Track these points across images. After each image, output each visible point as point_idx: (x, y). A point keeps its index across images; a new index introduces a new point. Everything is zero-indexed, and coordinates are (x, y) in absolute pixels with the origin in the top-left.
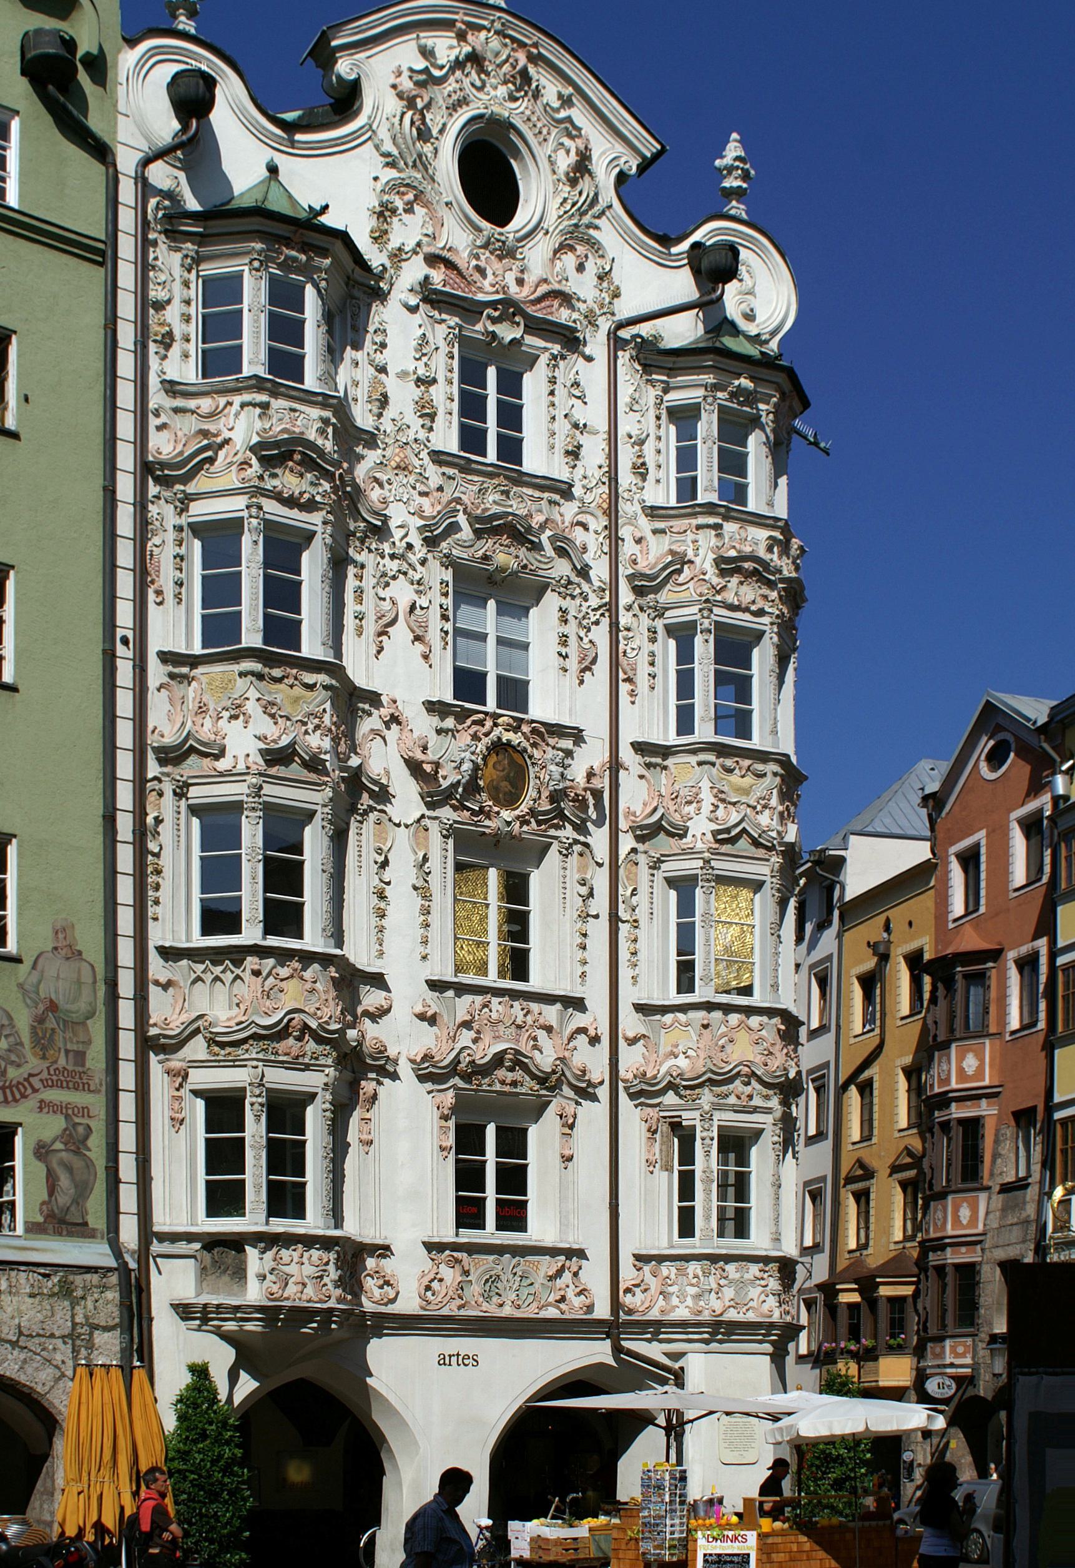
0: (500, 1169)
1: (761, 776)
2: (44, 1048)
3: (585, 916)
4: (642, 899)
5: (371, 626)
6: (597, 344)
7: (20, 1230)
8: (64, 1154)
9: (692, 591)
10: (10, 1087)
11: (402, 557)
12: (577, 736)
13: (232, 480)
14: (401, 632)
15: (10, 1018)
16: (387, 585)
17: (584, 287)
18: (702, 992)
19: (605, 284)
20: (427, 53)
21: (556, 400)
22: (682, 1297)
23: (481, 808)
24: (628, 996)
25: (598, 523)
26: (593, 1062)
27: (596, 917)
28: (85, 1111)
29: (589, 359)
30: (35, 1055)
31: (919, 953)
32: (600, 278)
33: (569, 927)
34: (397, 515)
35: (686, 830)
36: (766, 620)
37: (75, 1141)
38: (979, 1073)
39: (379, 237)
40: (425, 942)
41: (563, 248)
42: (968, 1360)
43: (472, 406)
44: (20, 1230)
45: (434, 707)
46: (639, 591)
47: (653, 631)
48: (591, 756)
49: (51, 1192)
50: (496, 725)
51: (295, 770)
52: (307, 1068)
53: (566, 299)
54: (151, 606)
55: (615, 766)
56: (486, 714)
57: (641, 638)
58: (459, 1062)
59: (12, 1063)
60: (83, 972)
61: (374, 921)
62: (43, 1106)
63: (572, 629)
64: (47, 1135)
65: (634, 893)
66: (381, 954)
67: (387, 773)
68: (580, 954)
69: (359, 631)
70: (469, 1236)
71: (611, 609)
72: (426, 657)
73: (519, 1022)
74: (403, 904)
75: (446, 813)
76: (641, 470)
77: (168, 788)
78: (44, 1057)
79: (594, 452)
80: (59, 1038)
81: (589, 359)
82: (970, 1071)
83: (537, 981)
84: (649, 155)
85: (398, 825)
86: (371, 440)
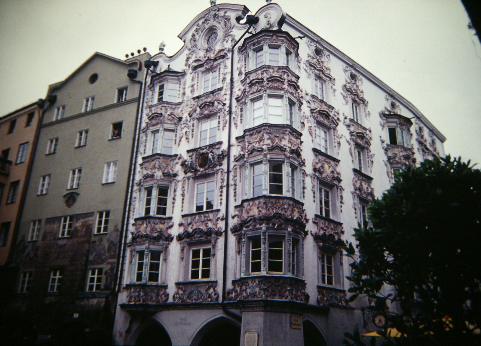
1: (260, 132)
3: (222, 187)
4: (238, 178)
11: (185, 124)
12: (220, 143)
14: (184, 139)
19: (233, 41)
20: (198, 25)
24: (232, 204)
25: (228, 92)
26: (221, 225)
27: (225, 186)
28: (114, 263)
32: (232, 41)
36: (262, 91)
37: (112, 269)
45: (188, 151)
46: (238, 101)
48: (225, 147)
51: (148, 179)
52: (142, 245)
55: (230, 146)
65: (235, 176)
66: (173, 213)
67: (178, 171)
68: (220, 198)
69: (175, 143)
72: (188, 142)
73: (203, 220)
75: (189, 174)
79: (228, 77)
84: (242, 9)
85: (179, 181)
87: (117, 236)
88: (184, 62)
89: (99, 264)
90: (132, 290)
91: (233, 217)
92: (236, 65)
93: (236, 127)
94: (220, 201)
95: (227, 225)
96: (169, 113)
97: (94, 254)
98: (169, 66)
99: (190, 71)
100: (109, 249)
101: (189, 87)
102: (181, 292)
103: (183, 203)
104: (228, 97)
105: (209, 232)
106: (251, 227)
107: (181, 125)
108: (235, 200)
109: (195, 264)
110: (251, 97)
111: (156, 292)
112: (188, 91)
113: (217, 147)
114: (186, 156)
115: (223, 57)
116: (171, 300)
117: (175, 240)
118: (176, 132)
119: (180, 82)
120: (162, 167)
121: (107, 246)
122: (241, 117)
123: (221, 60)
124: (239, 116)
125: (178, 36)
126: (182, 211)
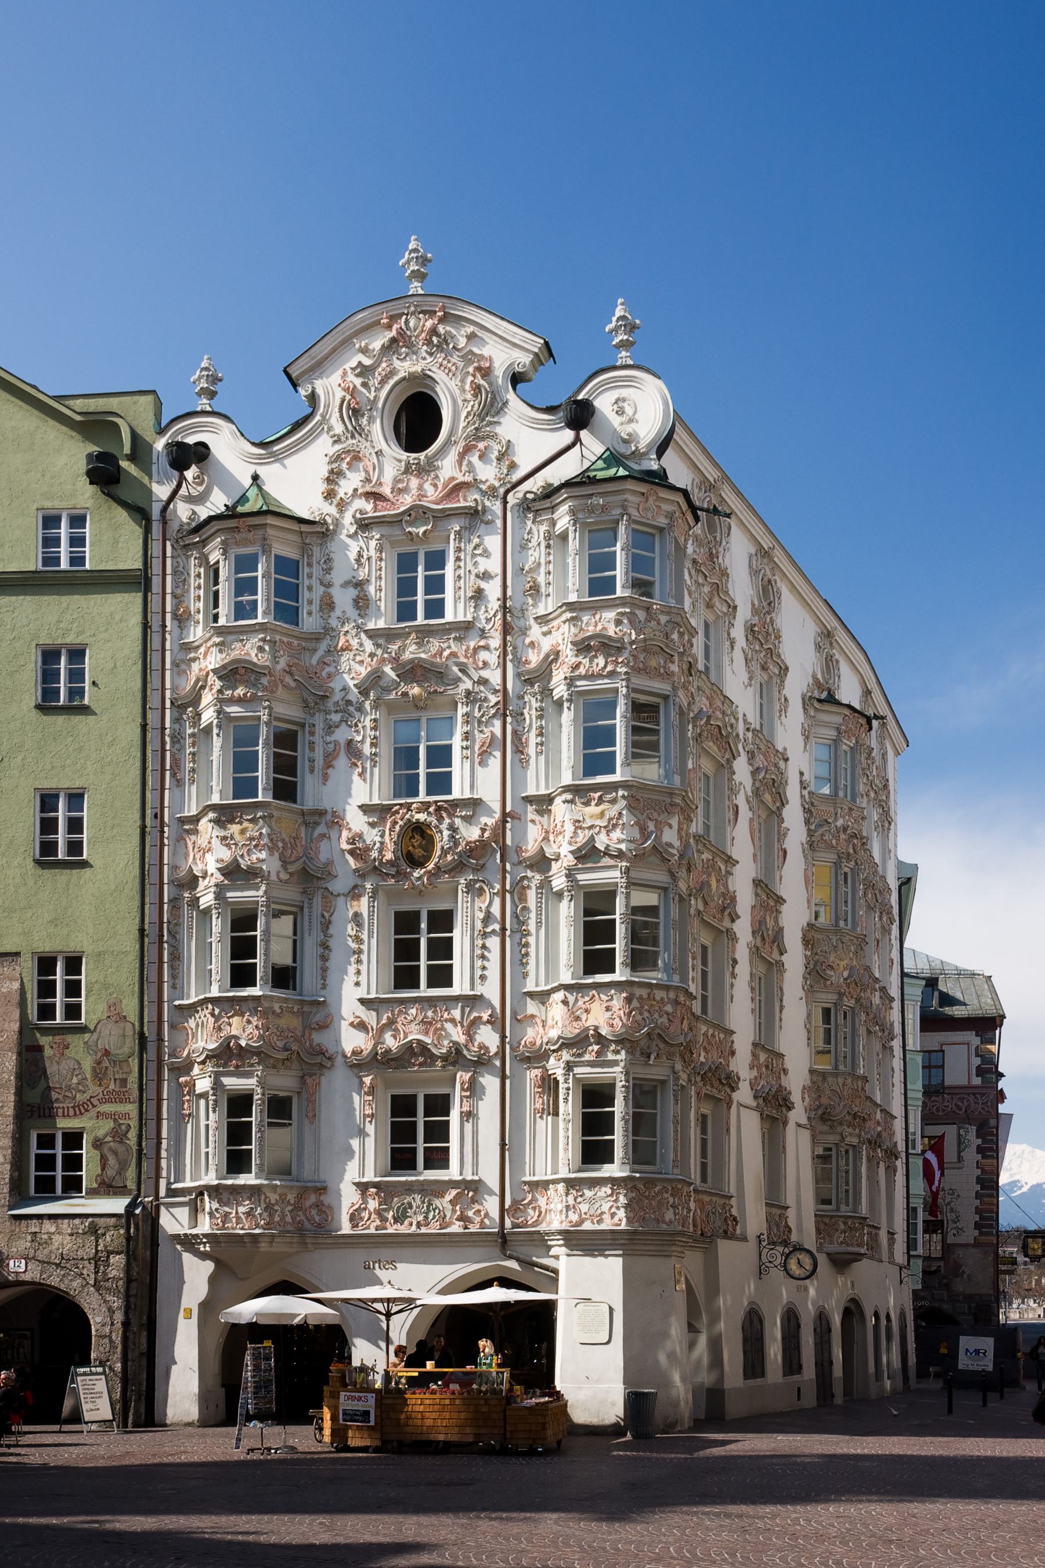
2: (100, 1079)
3: (485, 935)
5: (319, 762)
8: (112, 1144)
10: (78, 1106)
11: (341, 711)
12: (475, 804)
15: (79, 1063)
16: (333, 732)
17: (488, 473)
21: (462, 564)
23: (398, 872)
28: (126, 1116)
30: (94, 1084)
37: (119, 1135)
41: (467, 450)
50: (409, 810)
56: (401, 805)
58: (377, 1054)
59: (80, 1091)
60: (127, 1029)
61: (320, 963)
62: (99, 1115)
64: (101, 1133)
66: (324, 986)
78: (100, 1085)
85: (339, 895)
87: (124, 1036)
88: (323, 487)
94: (478, 973)
96: (282, 663)
98: (255, 478)
99: (348, 523)
100: (99, 1075)
101: (346, 584)
104: (492, 658)
105: (456, 1057)
106: (587, 1057)
107: (327, 712)
111: (292, 1202)
115: (475, 516)
119: (310, 556)
120: (280, 844)
122: (541, 734)
125: (285, 371)
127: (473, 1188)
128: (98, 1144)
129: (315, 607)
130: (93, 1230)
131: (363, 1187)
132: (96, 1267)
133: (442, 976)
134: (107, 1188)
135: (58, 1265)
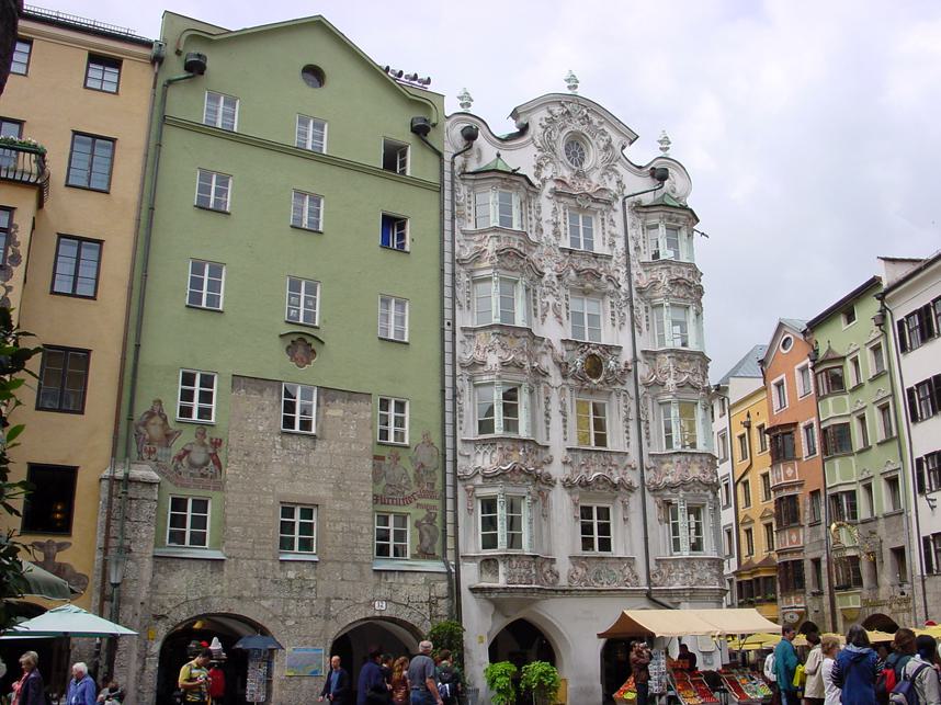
0: (599, 525)
3: (627, 420)
6: (618, 205)
7: (408, 557)
9: (661, 292)
12: (620, 348)
13: (487, 264)
14: (550, 314)
17: (612, 186)
18: (677, 448)
22: (677, 577)
25: (623, 270)
26: (633, 478)
29: (615, 210)
31: (763, 426)
33: (621, 425)
34: (547, 271)
35: (665, 383)
37: (431, 520)
38: (794, 476)
39: (537, 176)
40: (565, 433)
42: (803, 605)
43: (575, 230)
44: (408, 557)
47: (646, 308)
49: (421, 541)
51: (512, 369)
53: (604, 190)
54: (457, 311)
57: (642, 312)
63: (616, 309)
64: (420, 517)
66: (548, 439)
69: (536, 315)
70: (588, 554)
71: (630, 300)
72: (561, 323)
74: (556, 420)
76: (637, 248)
77: (465, 378)
79: (620, 243)
80: (425, 478)
81: (615, 210)
82: (790, 475)
83: (610, 446)
86: (536, 245)
89: (398, 504)
90: (514, 563)
91: (648, 469)
92: (631, 232)
93: (640, 332)
95: (642, 478)
97: (384, 482)
98: (499, 155)
100: (418, 480)
102: (580, 570)
103: (565, 426)
105: (621, 484)
106: (692, 492)
108: (649, 444)
109: (587, 529)
110: (673, 300)
112: (548, 229)
113: (615, 353)
114: (559, 349)
116: (563, 582)
117: (559, 486)
118: (534, 295)
121: (411, 472)
123: (604, 207)
124: (644, 319)
126: (565, 440)
127: (630, 561)
128: (418, 524)
129: (534, 230)
130: (427, 582)
131: (574, 559)
132: (430, 608)
133: (601, 440)
134: (425, 554)
135: (407, 606)
